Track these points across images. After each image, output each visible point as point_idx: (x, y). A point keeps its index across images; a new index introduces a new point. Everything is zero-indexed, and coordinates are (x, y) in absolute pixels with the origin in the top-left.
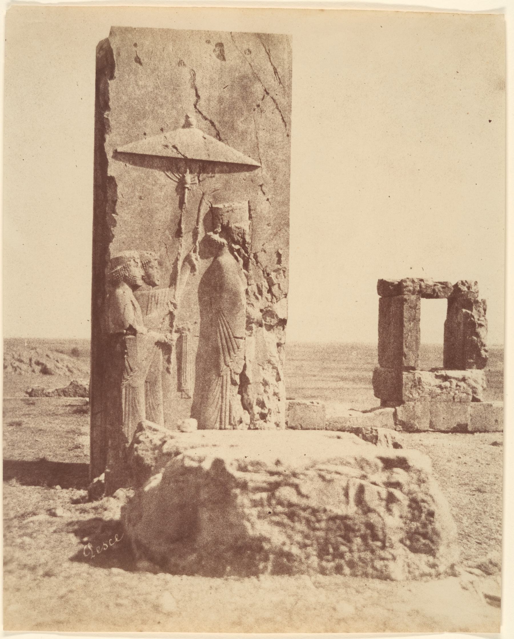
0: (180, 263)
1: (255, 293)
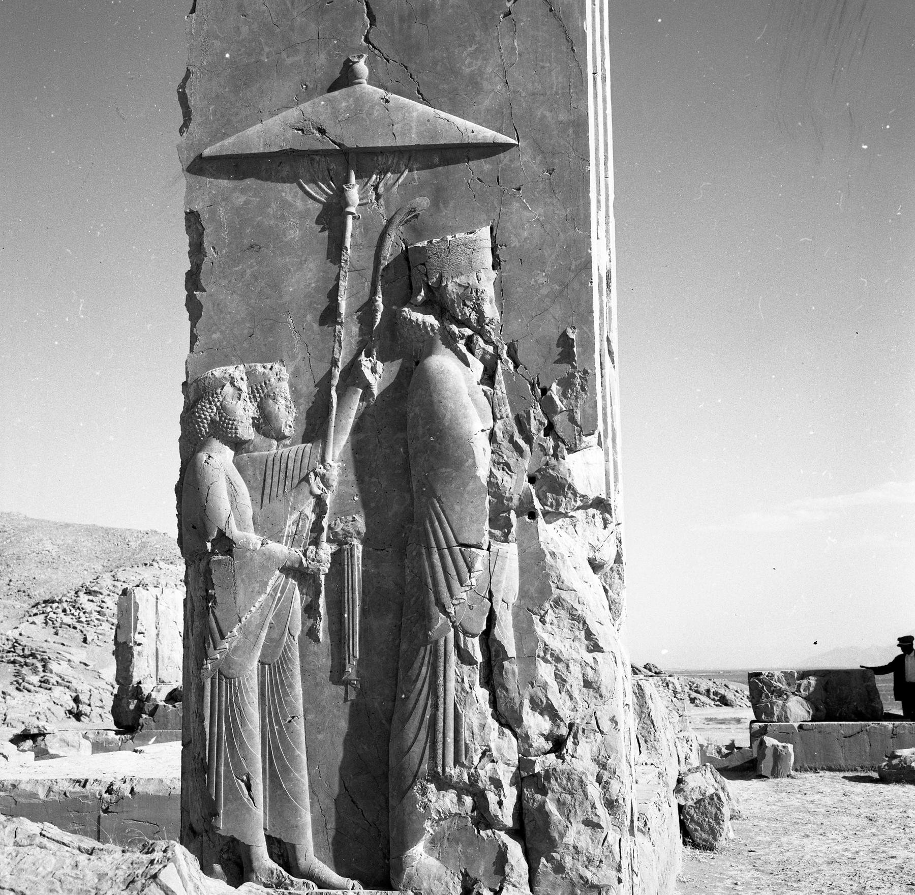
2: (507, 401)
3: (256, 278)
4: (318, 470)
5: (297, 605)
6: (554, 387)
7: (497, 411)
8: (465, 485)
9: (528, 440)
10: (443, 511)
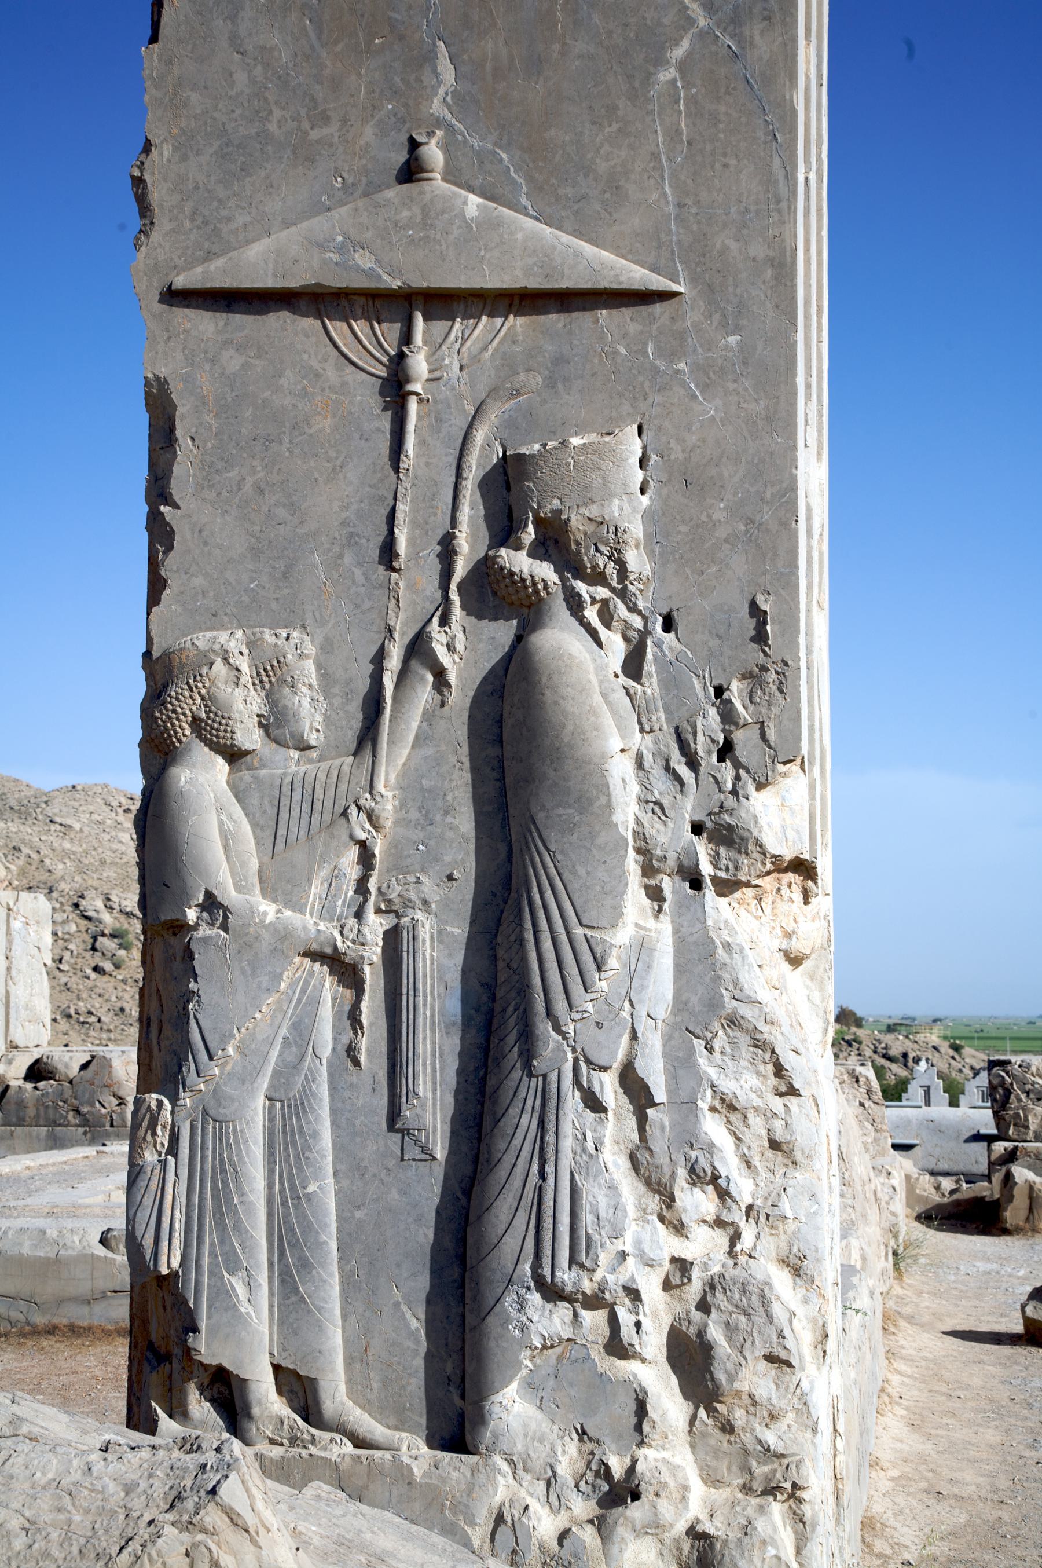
1: (668, 761)
2: (660, 704)
3: (261, 491)
4: (362, 802)
5: (327, 1013)
6: (735, 686)
7: (644, 720)
8: (592, 836)
9: (693, 764)
10: (559, 874)
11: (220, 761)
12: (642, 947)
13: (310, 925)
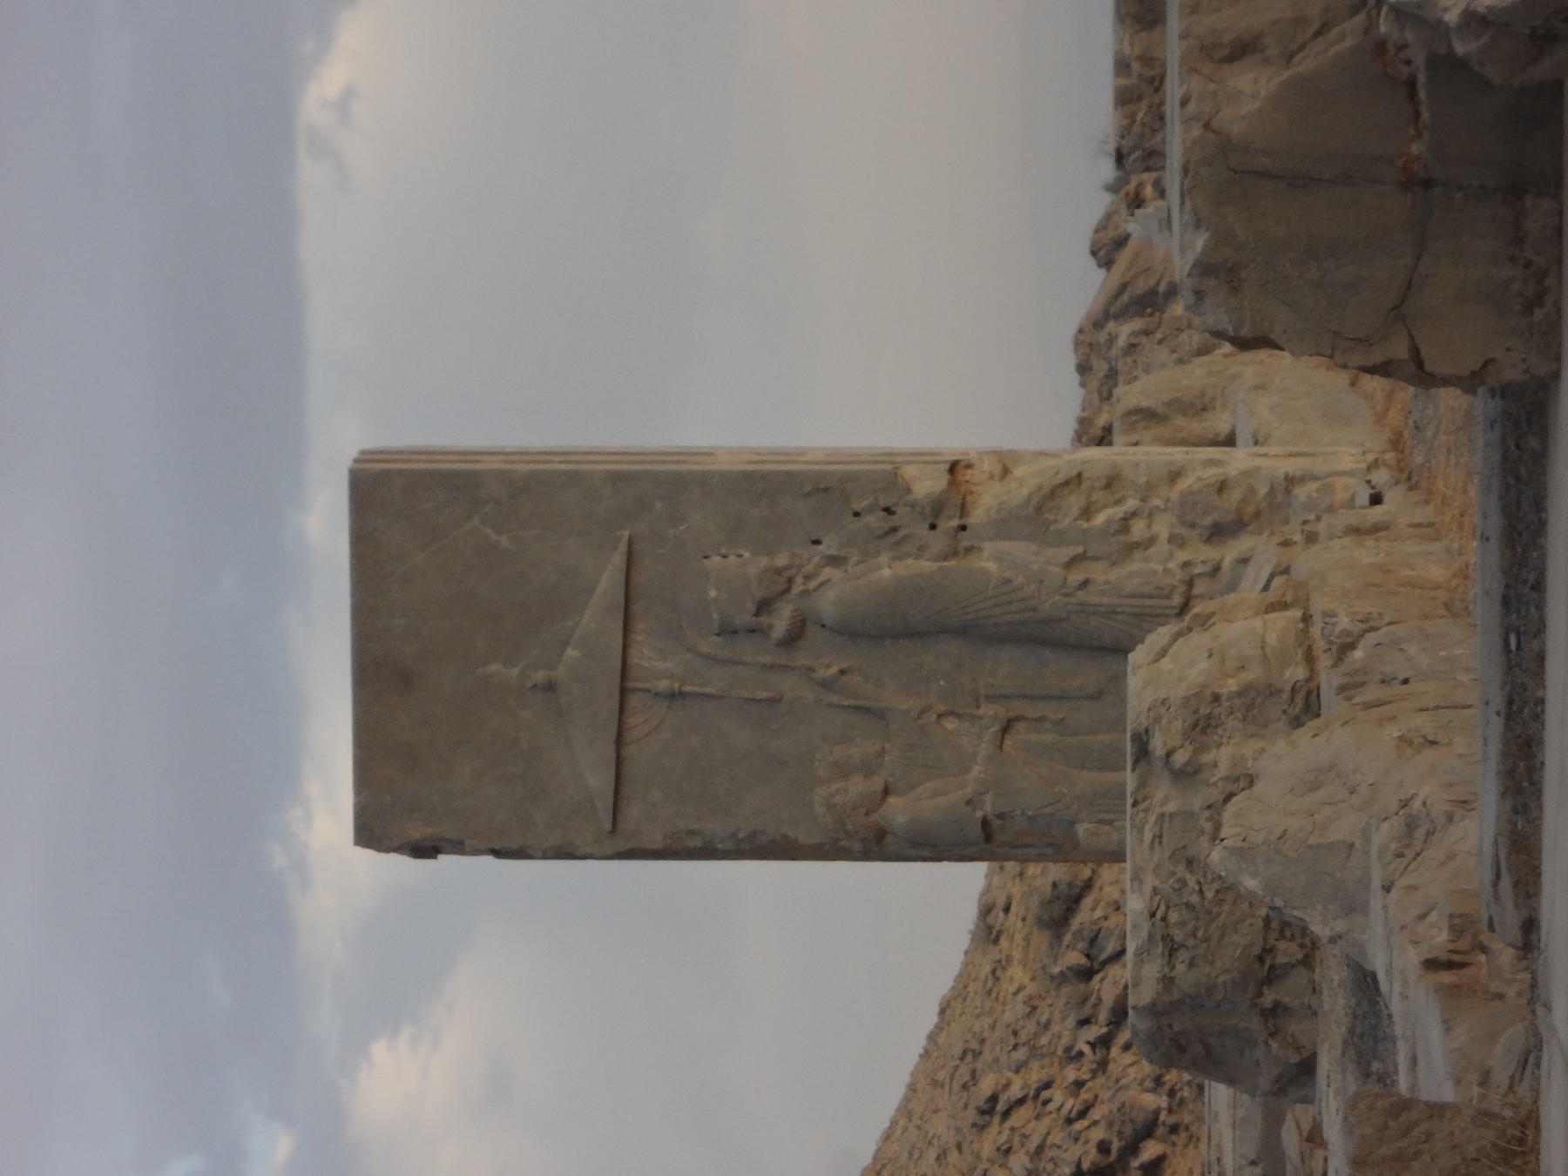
0: (835, 699)
9: (895, 529)
11: (891, 800)
12: (998, 558)
13: (985, 748)
